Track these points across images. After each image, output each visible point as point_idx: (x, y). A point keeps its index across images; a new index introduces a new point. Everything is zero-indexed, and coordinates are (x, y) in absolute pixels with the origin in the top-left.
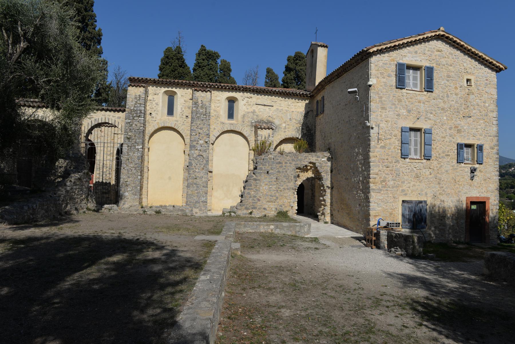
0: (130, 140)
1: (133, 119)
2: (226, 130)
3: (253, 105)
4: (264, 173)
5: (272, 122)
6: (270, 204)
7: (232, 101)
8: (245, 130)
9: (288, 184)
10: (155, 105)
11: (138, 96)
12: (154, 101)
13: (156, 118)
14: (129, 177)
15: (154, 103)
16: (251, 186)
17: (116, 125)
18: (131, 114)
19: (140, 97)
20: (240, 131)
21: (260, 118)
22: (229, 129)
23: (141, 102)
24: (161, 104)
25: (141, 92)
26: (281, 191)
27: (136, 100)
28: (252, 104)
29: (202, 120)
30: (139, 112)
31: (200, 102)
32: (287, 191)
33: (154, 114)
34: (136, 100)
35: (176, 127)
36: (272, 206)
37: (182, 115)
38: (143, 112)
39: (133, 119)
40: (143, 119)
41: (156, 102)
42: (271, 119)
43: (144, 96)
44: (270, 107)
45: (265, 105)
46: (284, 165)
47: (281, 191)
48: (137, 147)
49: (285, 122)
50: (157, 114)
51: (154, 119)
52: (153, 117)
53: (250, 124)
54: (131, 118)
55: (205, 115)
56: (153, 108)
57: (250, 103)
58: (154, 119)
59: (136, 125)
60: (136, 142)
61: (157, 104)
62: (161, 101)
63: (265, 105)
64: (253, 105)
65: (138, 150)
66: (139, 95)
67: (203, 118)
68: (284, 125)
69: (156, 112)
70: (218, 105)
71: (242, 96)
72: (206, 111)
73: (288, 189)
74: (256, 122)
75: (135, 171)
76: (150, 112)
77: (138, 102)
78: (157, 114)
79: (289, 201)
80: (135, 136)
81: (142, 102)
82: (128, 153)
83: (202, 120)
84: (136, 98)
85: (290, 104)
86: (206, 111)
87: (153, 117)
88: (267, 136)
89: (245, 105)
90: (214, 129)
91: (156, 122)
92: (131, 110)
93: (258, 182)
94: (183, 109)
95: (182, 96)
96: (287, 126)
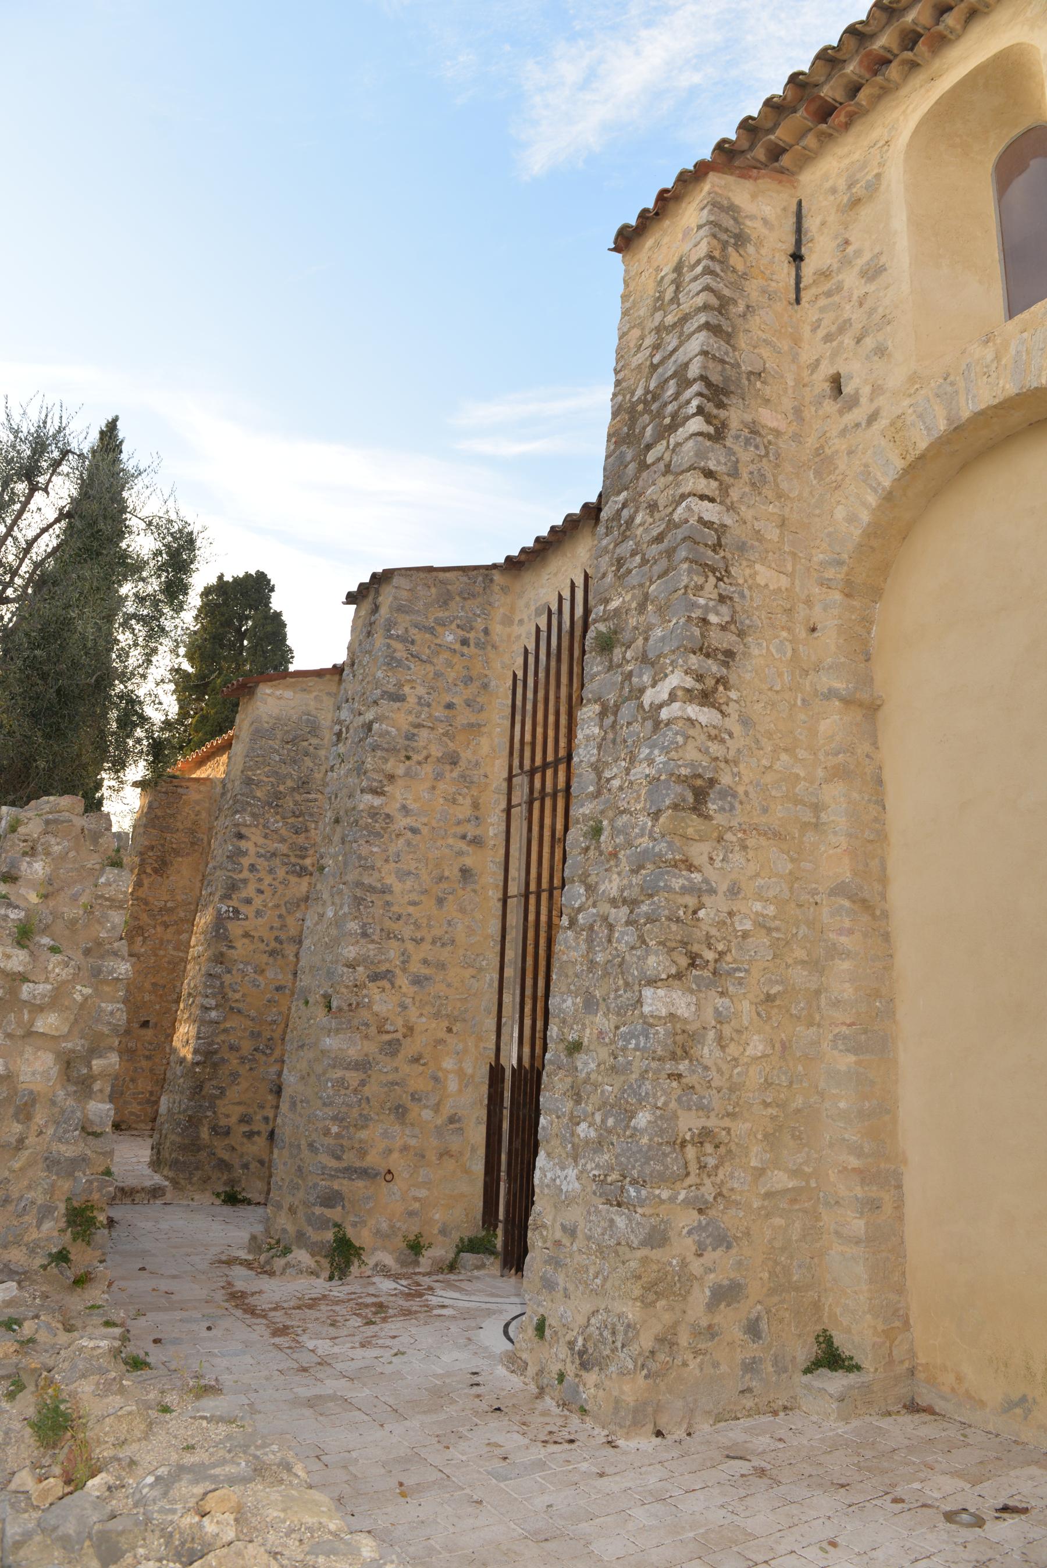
0: (617, 652)
1: (643, 466)
12: (846, 262)
13: (877, 390)
14: (590, 1004)
15: (850, 279)
23: (686, 307)
33: (858, 377)
39: (643, 466)
40: (696, 424)
48: (648, 698)
50: (881, 351)
54: (632, 467)
58: (858, 414)
59: (653, 507)
60: (644, 659)
62: (900, 221)
65: (657, 724)
66: (678, 269)
69: (869, 342)
75: (625, 936)
76: (826, 370)
77: (670, 320)
80: (642, 608)
81: (693, 297)
82: (597, 768)
91: (883, 423)
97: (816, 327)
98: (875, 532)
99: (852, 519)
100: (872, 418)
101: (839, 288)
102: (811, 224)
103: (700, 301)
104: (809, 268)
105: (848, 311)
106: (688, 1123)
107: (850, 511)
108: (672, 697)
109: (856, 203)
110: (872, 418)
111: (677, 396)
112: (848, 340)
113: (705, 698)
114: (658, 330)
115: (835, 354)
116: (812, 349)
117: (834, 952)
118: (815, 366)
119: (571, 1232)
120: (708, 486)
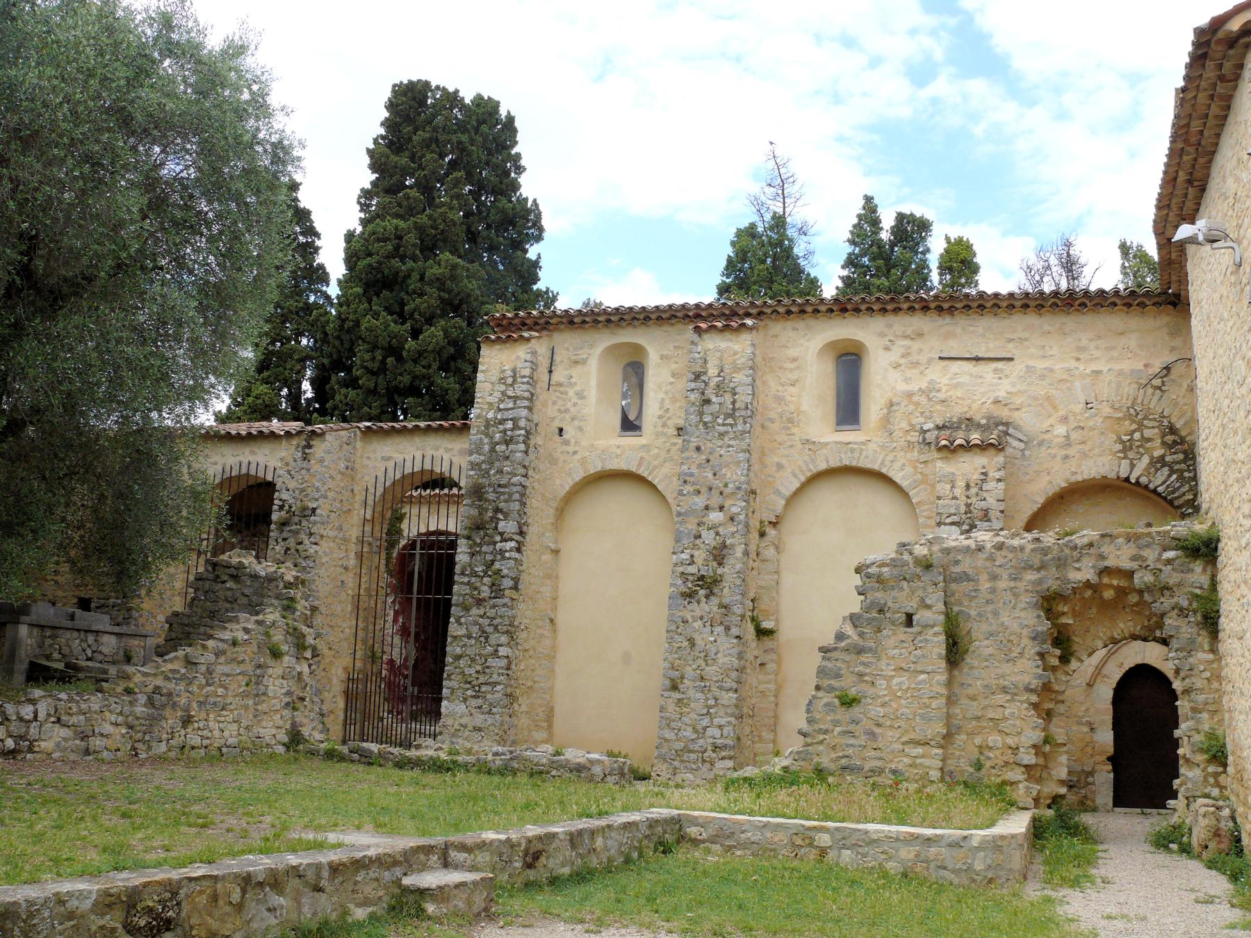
2: (823, 466)
3: (930, 361)
4: (893, 623)
5: (1007, 424)
6: (920, 750)
7: (849, 362)
8: (897, 465)
9: (1007, 668)
10: (575, 400)
11: (509, 373)
12: (571, 385)
15: (571, 392)
16: (838, 676)
17: (455, 476)
18: (487, 435)
19: (514, 377)
20: (876, 467)
21: (956, 412)
22: (834, 463)
24: (593, 394)
25: (518, 358)
26: (973, 698)
27: (503, 388)
28: (923, 359)
29: (722, 435)
30: (509, 425)
31: (712, 371)
32: (1000, 698)
34: (503, 388)
35: (643, 472)
36: (927, 762)
37: (664, 425)
38: (522, 423)
40: (522, 447)
41: (578, 388)
42: (1004, 414)
43: (527, 372)
44: (1000, 365)
45: (977, 359)
46: (985, 585)
47: (973, 698)
48: (499, 546)
49: (1064, 420)
50: (580, 429)
51: (571, 449)
52: (567, 443)
53: (914, 437)
55: (731, 415)
56: (567, 411)
57: (914, 358)
58: (571, 449)
61: (580, 395)
63: (977, 359)
64: (930, 361)
67: (722, 429)
68: (1061, 430)
69: (576, 423)
70: (794, 376)
71: (882, 335)
72: (734, 403)
73: (1005, 690)
74: (938, 428)
76: (557, 424)
77: (510, 393)
78: (580, 429)
79: (1010, 741)
83: (722, 435)
84: (502, 380)
85: (1084, 342)
86: (734, 403)
87: (567, 443)
88: (976, 476)
89: (897, 366)
90: (780, 467)
91: (577, 457)
92: (487, 421)
93: (866, 658)
94: (667, 404)
95: (662, 357)
96: (1074, 436)
97: (554, 403)
98: (568, 492)
99: (562, 485)
100: (575, 453)
101: (566, 393)
102: (557, 358)
103: (526, 394)
104: (557, 377)
105: (569, 405)
106: (509, 690)
107: (563, 484)
108: (511, 550)
109: (576, 362)
110: (575, 453)
111: (512, 430)
112: (568, 416)
113: (518, 550)
114: (503, 393)
115: (562, 420)
116: (551, 411)
117: (542, 636)
118: (553, 419)
119: (465, 727)
120: (522, 471)
